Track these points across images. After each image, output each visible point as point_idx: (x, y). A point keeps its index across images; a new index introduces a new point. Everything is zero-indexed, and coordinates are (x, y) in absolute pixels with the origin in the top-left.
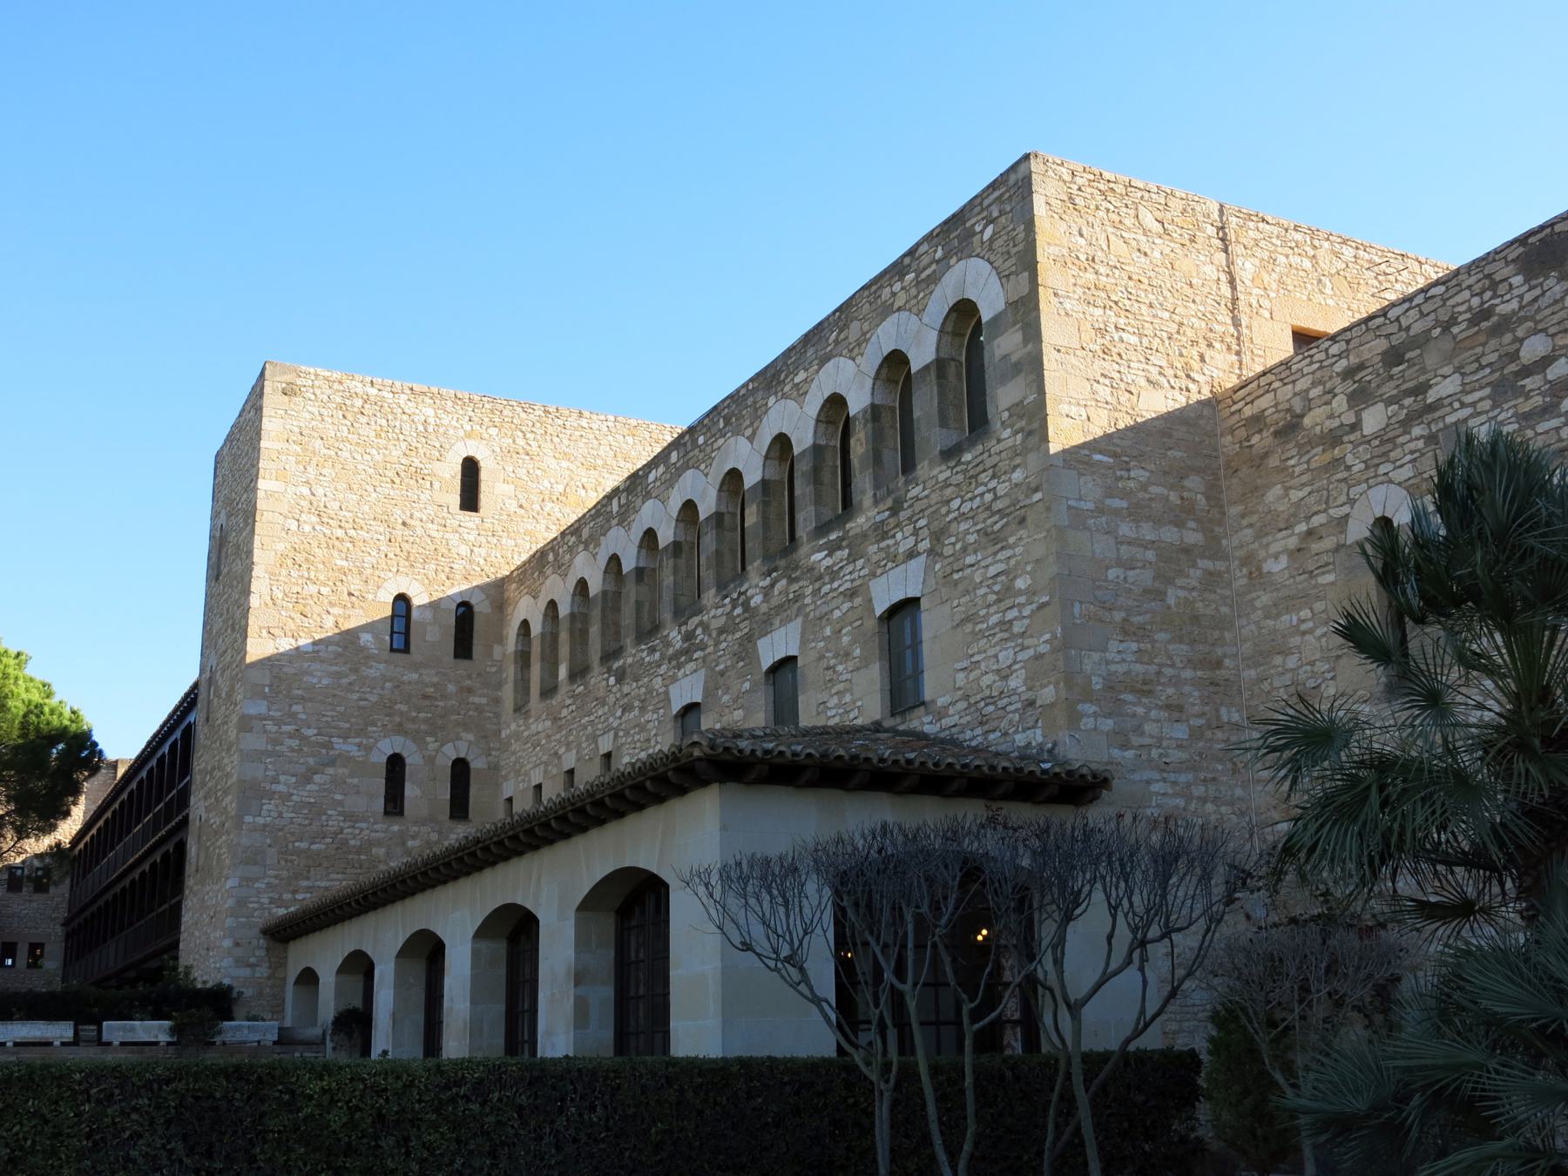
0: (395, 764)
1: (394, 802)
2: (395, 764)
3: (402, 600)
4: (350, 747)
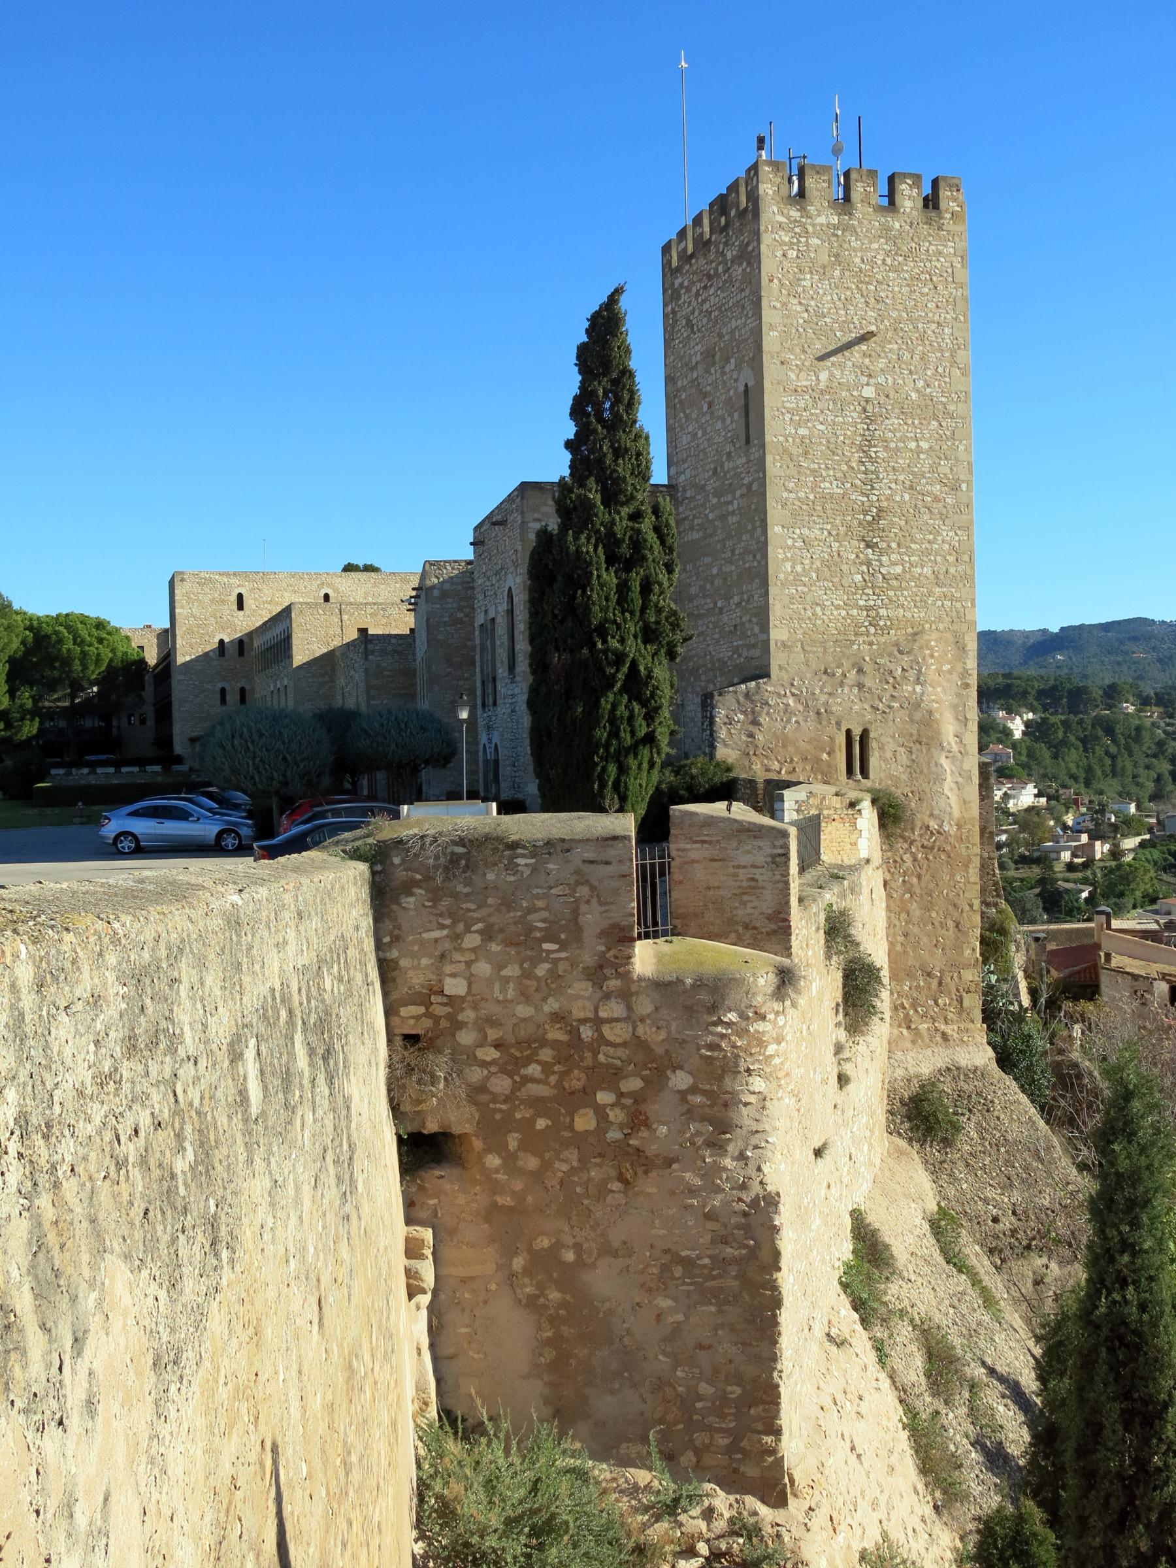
0: (223, 691)
1: (223, 701)
2: (223, 691)
3: (221, 642)
4: (209, 686)
